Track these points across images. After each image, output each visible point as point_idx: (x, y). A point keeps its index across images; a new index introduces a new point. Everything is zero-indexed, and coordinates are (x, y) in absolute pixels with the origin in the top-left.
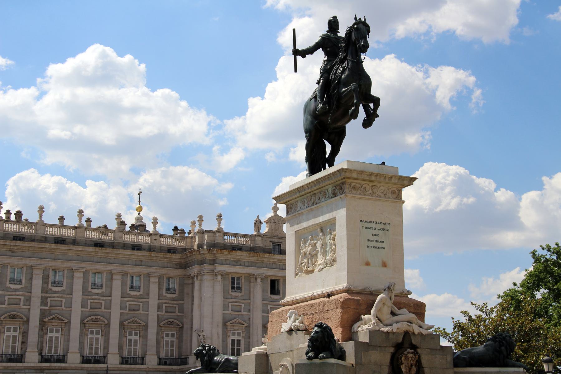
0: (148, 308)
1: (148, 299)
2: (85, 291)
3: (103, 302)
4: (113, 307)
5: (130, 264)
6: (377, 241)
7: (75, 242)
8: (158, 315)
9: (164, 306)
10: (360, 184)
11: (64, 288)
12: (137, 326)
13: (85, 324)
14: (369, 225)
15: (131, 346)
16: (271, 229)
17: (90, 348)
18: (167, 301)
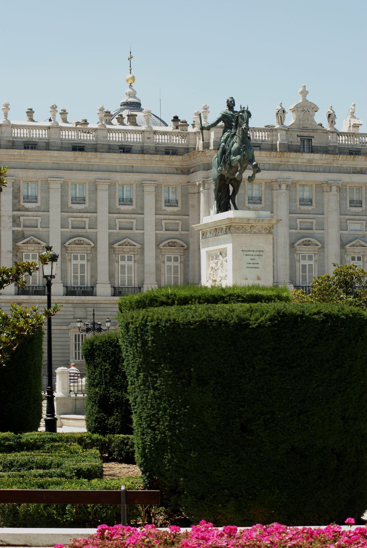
0: (143, 226)
1: (143, 214)
2: (64, 209)
3: (87, 220)
4: (99, 226)
5: (118, 171)
6: (253, 264)
7: (48, 147)
8: (156, 234)
9: (163, 222)
10: (242, 226)
11: (39, 204)
12: (130, 248)
13: (65, 247)
14: (248, 253)
15: (125, 274)
16: (298, 120)
17: (74, 276)
18: (167, 217)
